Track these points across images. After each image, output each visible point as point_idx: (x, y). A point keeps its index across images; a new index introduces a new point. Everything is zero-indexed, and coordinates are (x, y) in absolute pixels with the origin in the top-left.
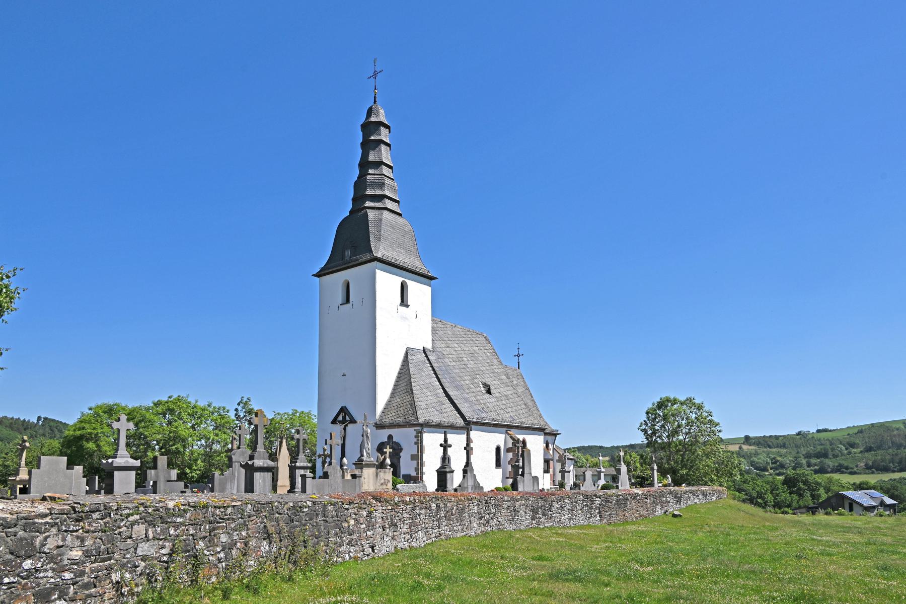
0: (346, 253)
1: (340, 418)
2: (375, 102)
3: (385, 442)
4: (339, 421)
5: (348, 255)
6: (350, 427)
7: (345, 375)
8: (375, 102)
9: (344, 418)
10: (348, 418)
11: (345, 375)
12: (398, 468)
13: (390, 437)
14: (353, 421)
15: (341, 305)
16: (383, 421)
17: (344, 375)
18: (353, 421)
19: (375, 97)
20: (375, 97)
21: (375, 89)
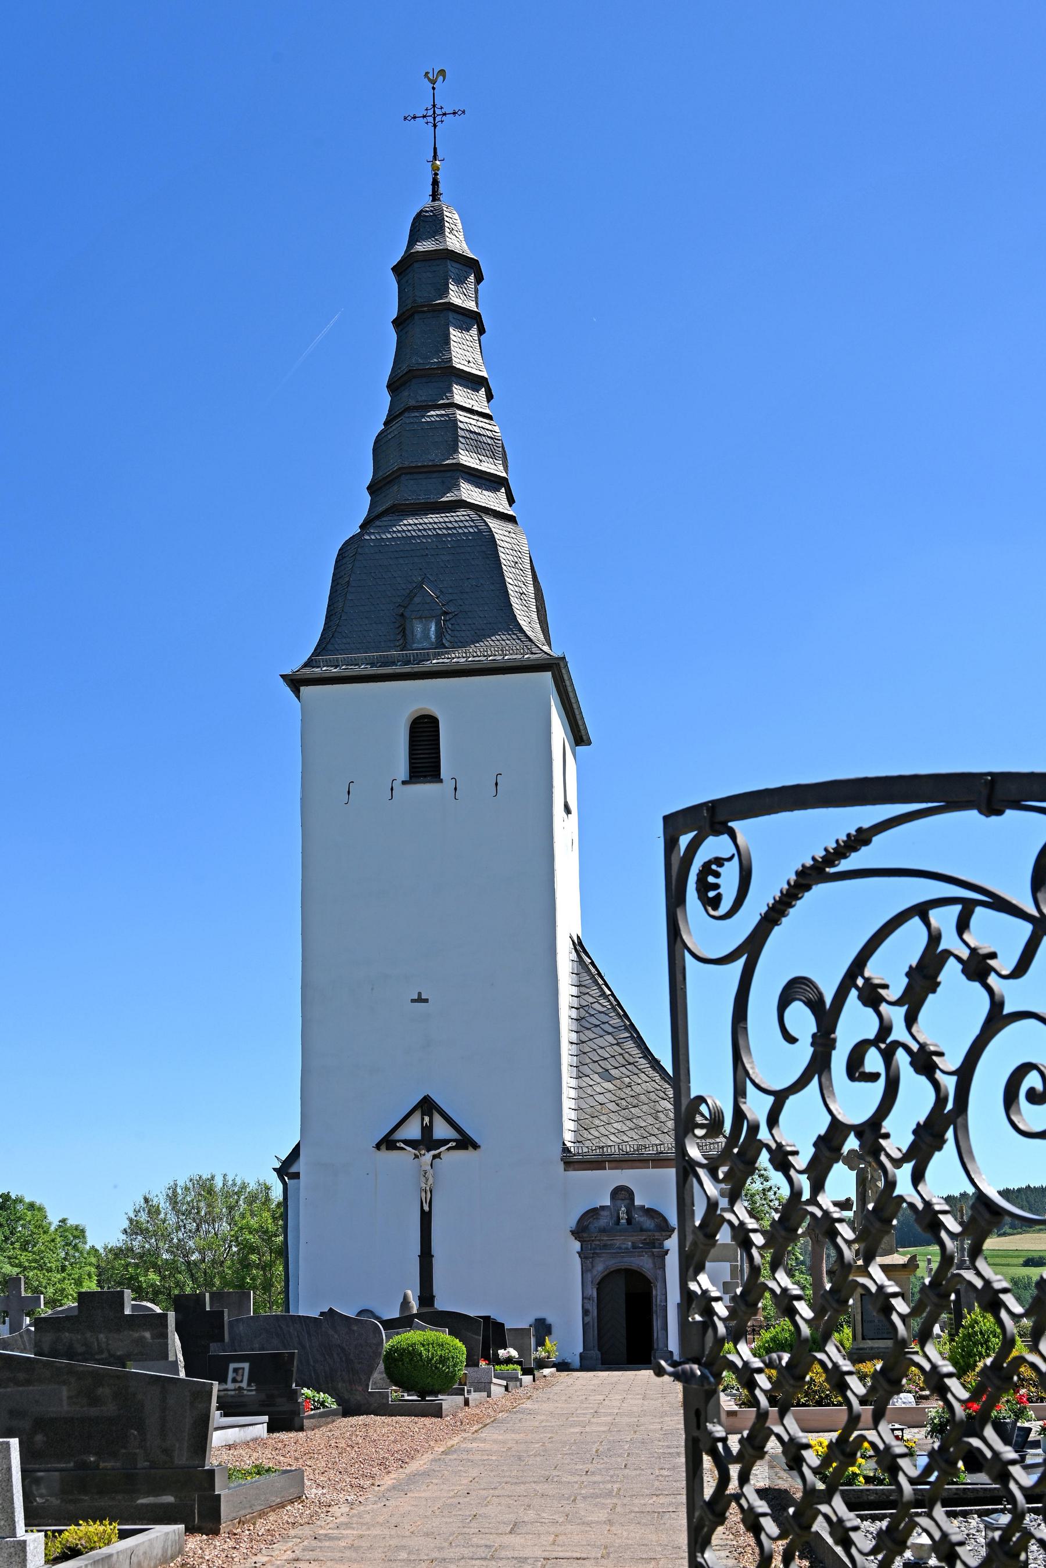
0: (418, 628)
1: (413, 1130)
2: (435, 196)
3: (603, 1208)
4: (408, 1143)
5: (427, 636)
6: (452, 1158)
7: (426, 1001)
8: (435, 196)
9: (427, 1130)
10: (441, 1130)
11: (426, 1001)
12: (659, 1285)
13: (620, 1193)
14: (465, 1142)
15: (404, 783)
16: (588, 1143)
17: (420, 1000)
18: (465, 1142)
19: (435, 183)
20: (435, 183)
21: (435, 157)
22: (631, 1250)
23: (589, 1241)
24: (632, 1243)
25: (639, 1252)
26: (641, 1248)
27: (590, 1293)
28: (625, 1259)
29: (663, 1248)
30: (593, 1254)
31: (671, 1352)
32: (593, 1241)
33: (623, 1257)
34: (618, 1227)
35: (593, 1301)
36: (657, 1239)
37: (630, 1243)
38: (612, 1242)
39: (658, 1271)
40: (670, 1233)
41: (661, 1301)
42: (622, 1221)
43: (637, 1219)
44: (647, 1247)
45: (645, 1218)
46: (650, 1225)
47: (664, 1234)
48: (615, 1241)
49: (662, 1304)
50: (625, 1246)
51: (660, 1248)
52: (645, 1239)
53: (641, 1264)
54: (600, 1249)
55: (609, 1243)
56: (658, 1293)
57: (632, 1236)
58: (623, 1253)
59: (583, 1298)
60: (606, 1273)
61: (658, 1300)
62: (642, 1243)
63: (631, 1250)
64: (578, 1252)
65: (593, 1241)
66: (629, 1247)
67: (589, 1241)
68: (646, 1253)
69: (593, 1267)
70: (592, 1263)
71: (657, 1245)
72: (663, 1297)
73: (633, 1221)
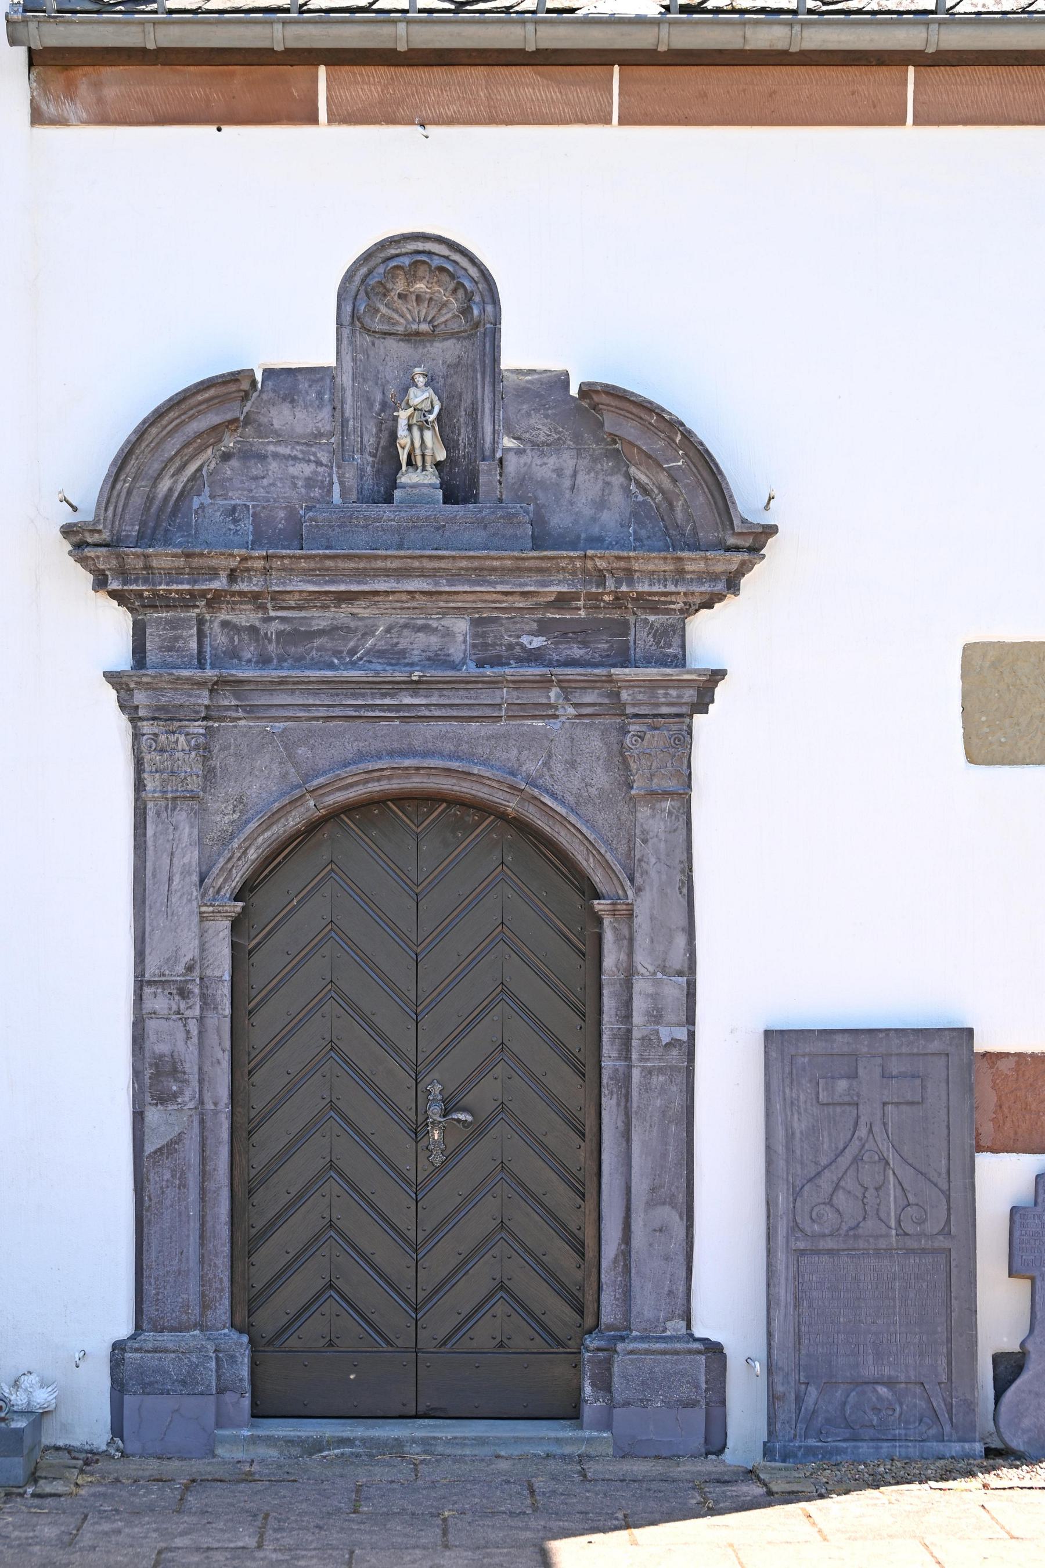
22: (470, 669)
23: (188, 601)
24: (476, 623)
25: (518, 684)
26: (534, 657)
27: (189, 951)
28: (424, 733)
29: (680, 661)
30: (215, 687)
31: (714, 1350)
32: (215, 600)
33: (410, 716)
34: (386, 511)
35: (207, 1001)
36: (647, 603)
37: (461, 626)
38: (341, 614)
39: (644, 812)
40: (725, 563)
41: (656, 1016)
42: (408, 478)
43: (512, 464)
44: (577, 652)
45: (568, 460)
46: (601, 504)
47: (694, 564)
48: (360, 609)
49: (665, 1034)
50: (434, 641)
51: (663, 662)
52: (562, 601)
53: (531, 767)
54: (264, 661)
55: (320, 619)
56: (643, 961)
57: (481, 573)
58: (414, 686)
59: (141, 983)
60: (294, 821)
61: (639, 1005)
62: (543, 628)
63: (470, 669)
64: (113, 678)
65: (215, 600)
66: (457, 650)
67: (188, 601)
68: (567, 688)
69: (209, 776)
70: (205, 751)
71: (641, 639)
72: (673, 990)
73: (487, 477)
